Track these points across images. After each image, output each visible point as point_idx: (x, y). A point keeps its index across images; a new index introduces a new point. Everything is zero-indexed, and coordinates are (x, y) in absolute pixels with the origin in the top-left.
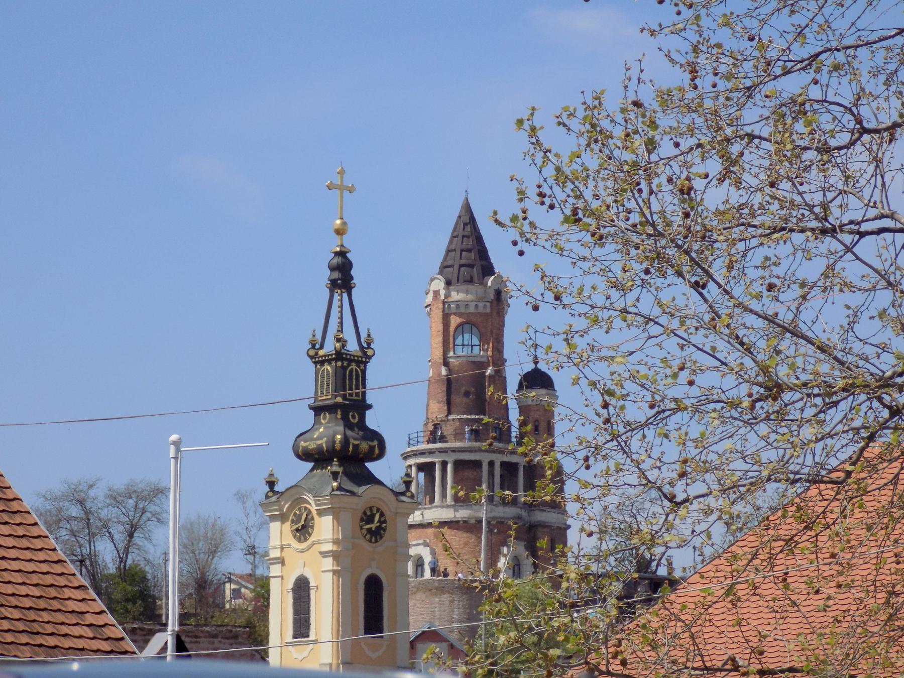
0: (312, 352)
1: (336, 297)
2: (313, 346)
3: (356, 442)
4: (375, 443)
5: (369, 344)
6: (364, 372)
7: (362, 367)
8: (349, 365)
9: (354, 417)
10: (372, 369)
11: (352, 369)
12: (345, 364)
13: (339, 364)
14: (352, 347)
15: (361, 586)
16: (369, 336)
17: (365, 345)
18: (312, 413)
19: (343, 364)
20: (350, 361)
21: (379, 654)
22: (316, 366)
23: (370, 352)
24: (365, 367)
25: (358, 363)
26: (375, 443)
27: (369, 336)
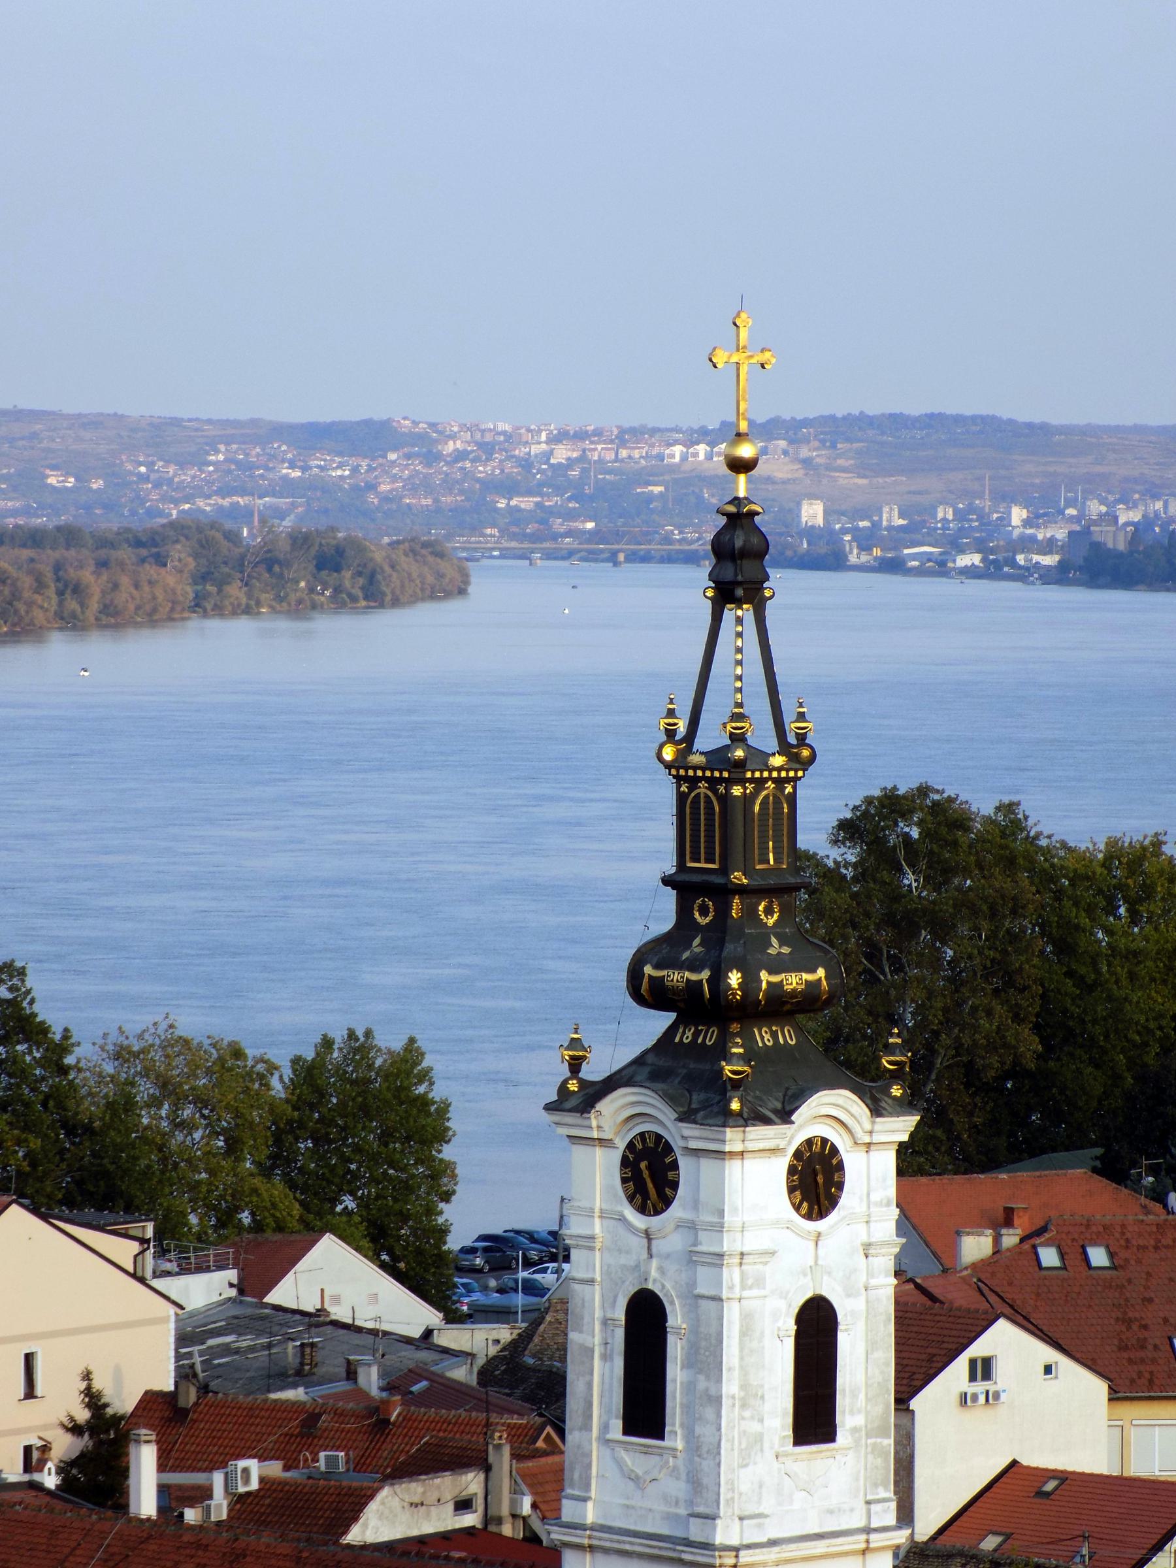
0: (669, 753)
1: (729, 614)
3: (775, 979)
4: (821, 973)
6: (792, 799)
7: (789, 789)
8: (757, 791)
9: (769, 911)
11: (767, 797)
12: (750, 787)
13: (737, 791)
14: (762, 736)
16: (801, 717)
17: (792, 740)
18: (671, 895)
19: (745, 788)
20: (761, 782)
23: (806, 753)
24: (795, 788)
25: (780, 782)
26: (821, 973)
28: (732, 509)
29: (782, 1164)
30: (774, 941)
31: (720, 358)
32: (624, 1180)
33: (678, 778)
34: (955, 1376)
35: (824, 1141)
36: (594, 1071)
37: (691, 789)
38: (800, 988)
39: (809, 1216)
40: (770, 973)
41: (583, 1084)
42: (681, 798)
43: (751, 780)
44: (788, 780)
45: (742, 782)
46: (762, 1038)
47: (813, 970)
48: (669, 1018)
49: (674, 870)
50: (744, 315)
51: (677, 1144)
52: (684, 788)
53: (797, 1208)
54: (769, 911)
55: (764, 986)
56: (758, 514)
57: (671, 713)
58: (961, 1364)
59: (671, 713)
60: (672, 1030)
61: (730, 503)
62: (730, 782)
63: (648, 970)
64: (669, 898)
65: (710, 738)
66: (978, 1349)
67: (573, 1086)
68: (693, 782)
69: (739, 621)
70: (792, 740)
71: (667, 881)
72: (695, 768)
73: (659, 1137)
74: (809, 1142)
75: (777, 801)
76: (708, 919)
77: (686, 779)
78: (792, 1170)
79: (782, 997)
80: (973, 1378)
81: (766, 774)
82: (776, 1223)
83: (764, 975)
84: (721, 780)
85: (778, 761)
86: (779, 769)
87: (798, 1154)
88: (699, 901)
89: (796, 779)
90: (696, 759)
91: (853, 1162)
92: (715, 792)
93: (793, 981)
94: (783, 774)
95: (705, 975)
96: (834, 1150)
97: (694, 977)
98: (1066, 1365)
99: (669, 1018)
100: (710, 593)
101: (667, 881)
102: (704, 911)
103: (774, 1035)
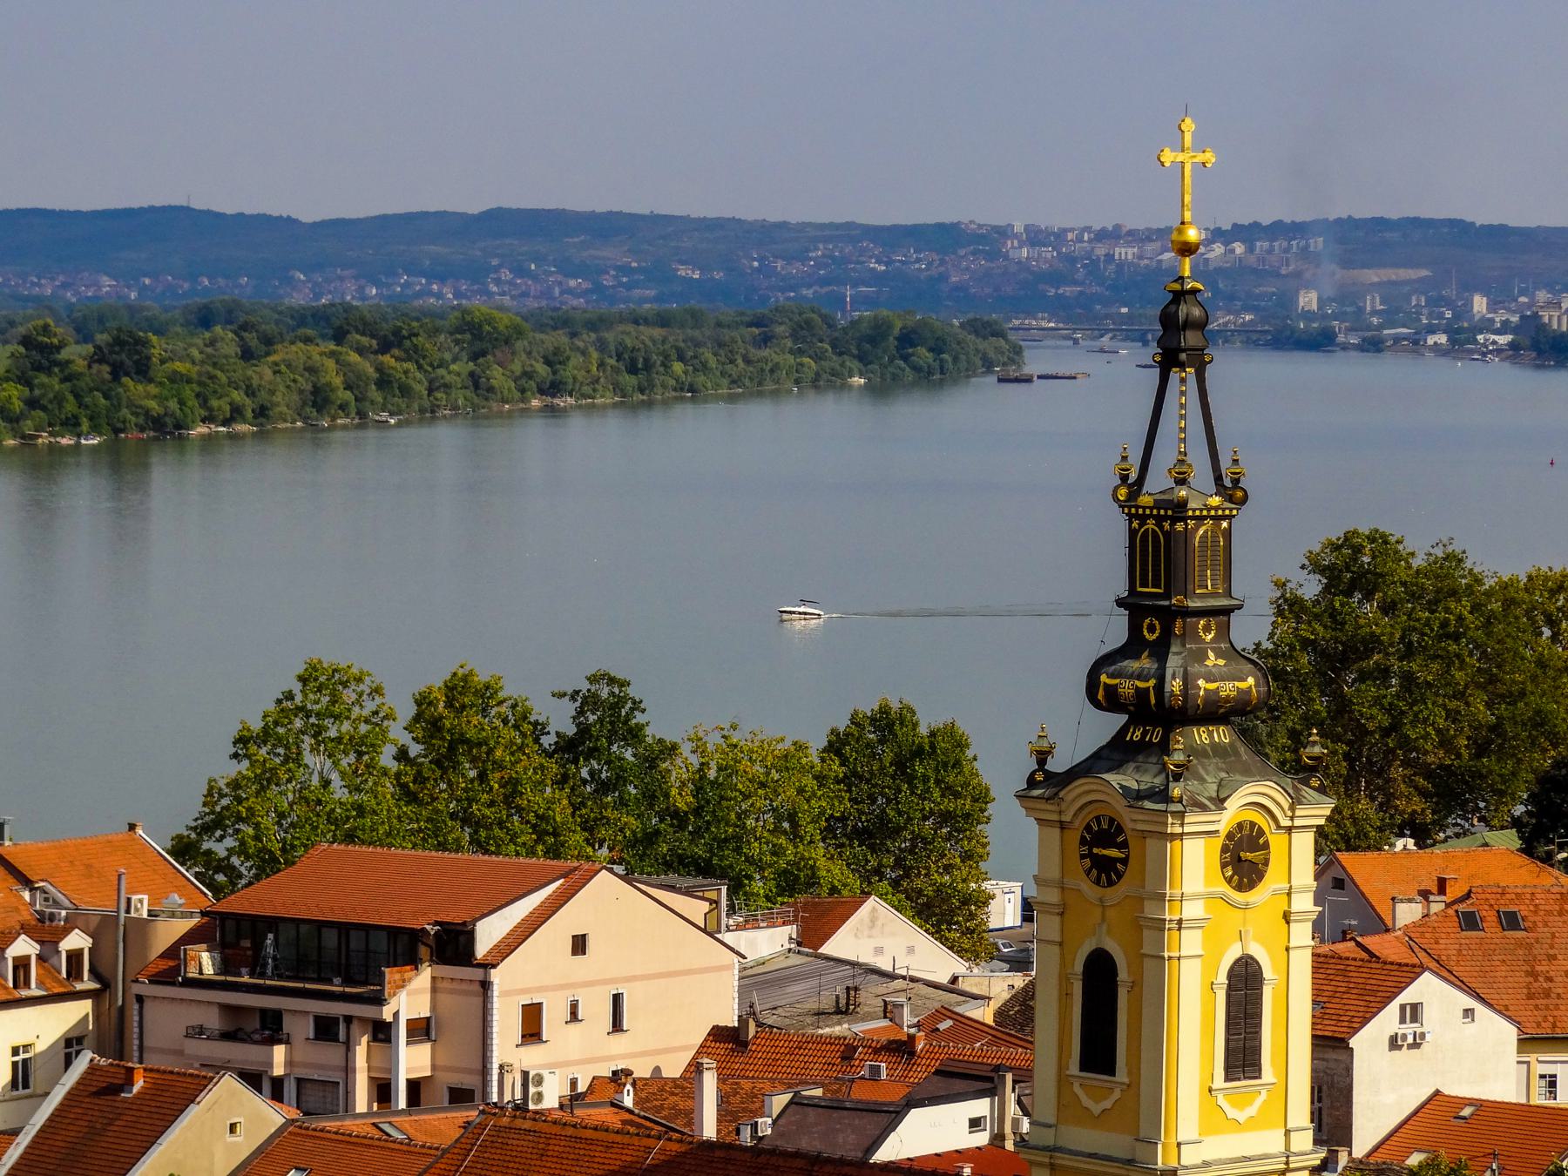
0: (1123, 493)
1: (1175, 375)
2: (1124, 478)
5: (1236, 482)
6: (1228, 534)
10: (1245, 524)
13: (1180, 527)
15: (1222, 978)
16: (1236, 461)
17: (1228, 483)
19: (1186, 524)
20: (1201, 519)
21: (1252, 1110)
22: (1131, 523)
23: (1240, 494)
25: (1217, 519)
26: (1251, 681)
27: (1236, 461)
28: (1177, 287)
29: (1218, 843)
30: (1211, 655)
31: (1168, 157)
32: (1083, 857)
33: (1131, 517)
34: (1387, 1021)
35: (1253, 824)
36: (1057, 765)
37: (1141, 526)
38: (1233, 694)
39: (1240, 888)
40: (1208, 681)
41: (1050, 776)
42: (1132, 533)
43: (1192, 518)
44: (1224, 517)
45: (1184, 519)
46: (1200, 736)
47: (1244, 680)
48: (1123, 718)
49: (1126, 593)
50: (1188, 121)
51: (1128, 826)
52: (1135, 524)
53: (1229, 881)
54: (1207, 629)
55: (1202, 693)
56: (1200, 291)
57: (1124, 458)
58: (1393, 1009)
59: (1124, 458)
60: (1123, 730)
61: (1175, 281)
62: (1174, 520)
63: (1104, 678)
64: (1122, 619)
65: (1158, 482)
66: (1407, 996)
67: (1039, 777)
68: (1143, 519)
69: (1183, 381)
70: (1228, 483)
71: (1120, 603)
72: (1144, 508)
73: (1112, 820)
74: (1240, 826)
75: (1215, 536)
76: (1156, 635)
77: (1137, 516)
78: (1225, 849)
79: (1219, 701)
80: (1402, 1021)
81: (1205, 513)
83: (1201, 682)
84: (1165, 518)
85: (1215, 501)
86: (1216, 509)
87: (1230, 836)
88: (1147, 621)
89: (1230, 517)
90: (1145, 500)
91: (1276, 841)
92: (1161, 528)
93: (1228, 689)
94: (1220, 512)
95: (1152, 683)
96: (1261, 832)
98: (1479, 1008)
99: (1123, 718)
100: (1158, 359)
101: (1120, 603)
102: (1151, 629)
103: (1210, 734)
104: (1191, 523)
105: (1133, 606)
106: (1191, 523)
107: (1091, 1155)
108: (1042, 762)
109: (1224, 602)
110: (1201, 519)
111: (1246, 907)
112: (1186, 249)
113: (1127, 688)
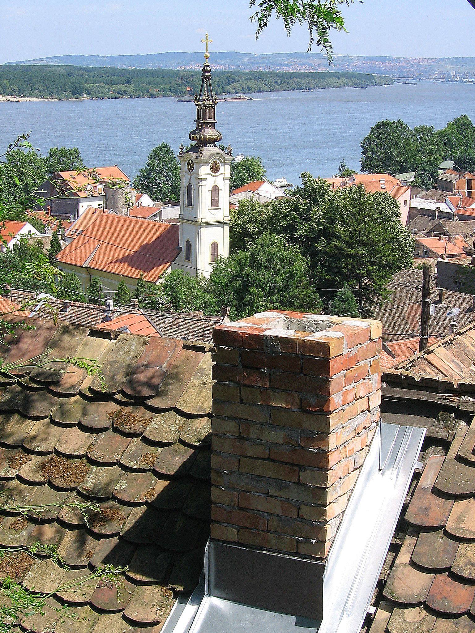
20: (208, 107)
33: (197, 106)
42: (197, 109)
68: (199, 106)
82: (208, 174)
84: (202, 106)
97: (197, 136)
102: (200, 126)
104: (206, 107)
105: (198, 122)
106: (206, 107)
107: (188, 220)
108: (182, 150)
109: (214, 121)
110: (208, 107)
111: (215, 176)
112: (207, 58)
113: (195, 136)
